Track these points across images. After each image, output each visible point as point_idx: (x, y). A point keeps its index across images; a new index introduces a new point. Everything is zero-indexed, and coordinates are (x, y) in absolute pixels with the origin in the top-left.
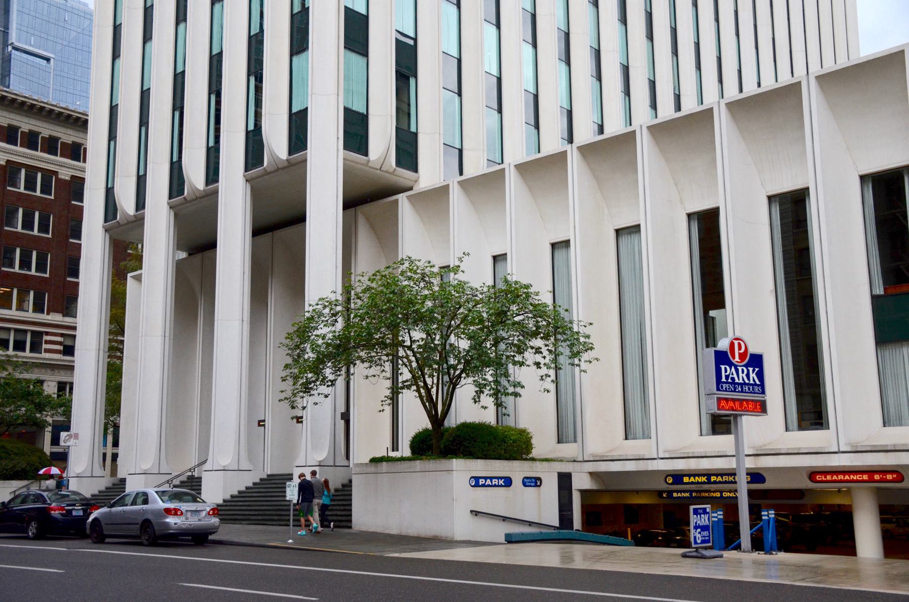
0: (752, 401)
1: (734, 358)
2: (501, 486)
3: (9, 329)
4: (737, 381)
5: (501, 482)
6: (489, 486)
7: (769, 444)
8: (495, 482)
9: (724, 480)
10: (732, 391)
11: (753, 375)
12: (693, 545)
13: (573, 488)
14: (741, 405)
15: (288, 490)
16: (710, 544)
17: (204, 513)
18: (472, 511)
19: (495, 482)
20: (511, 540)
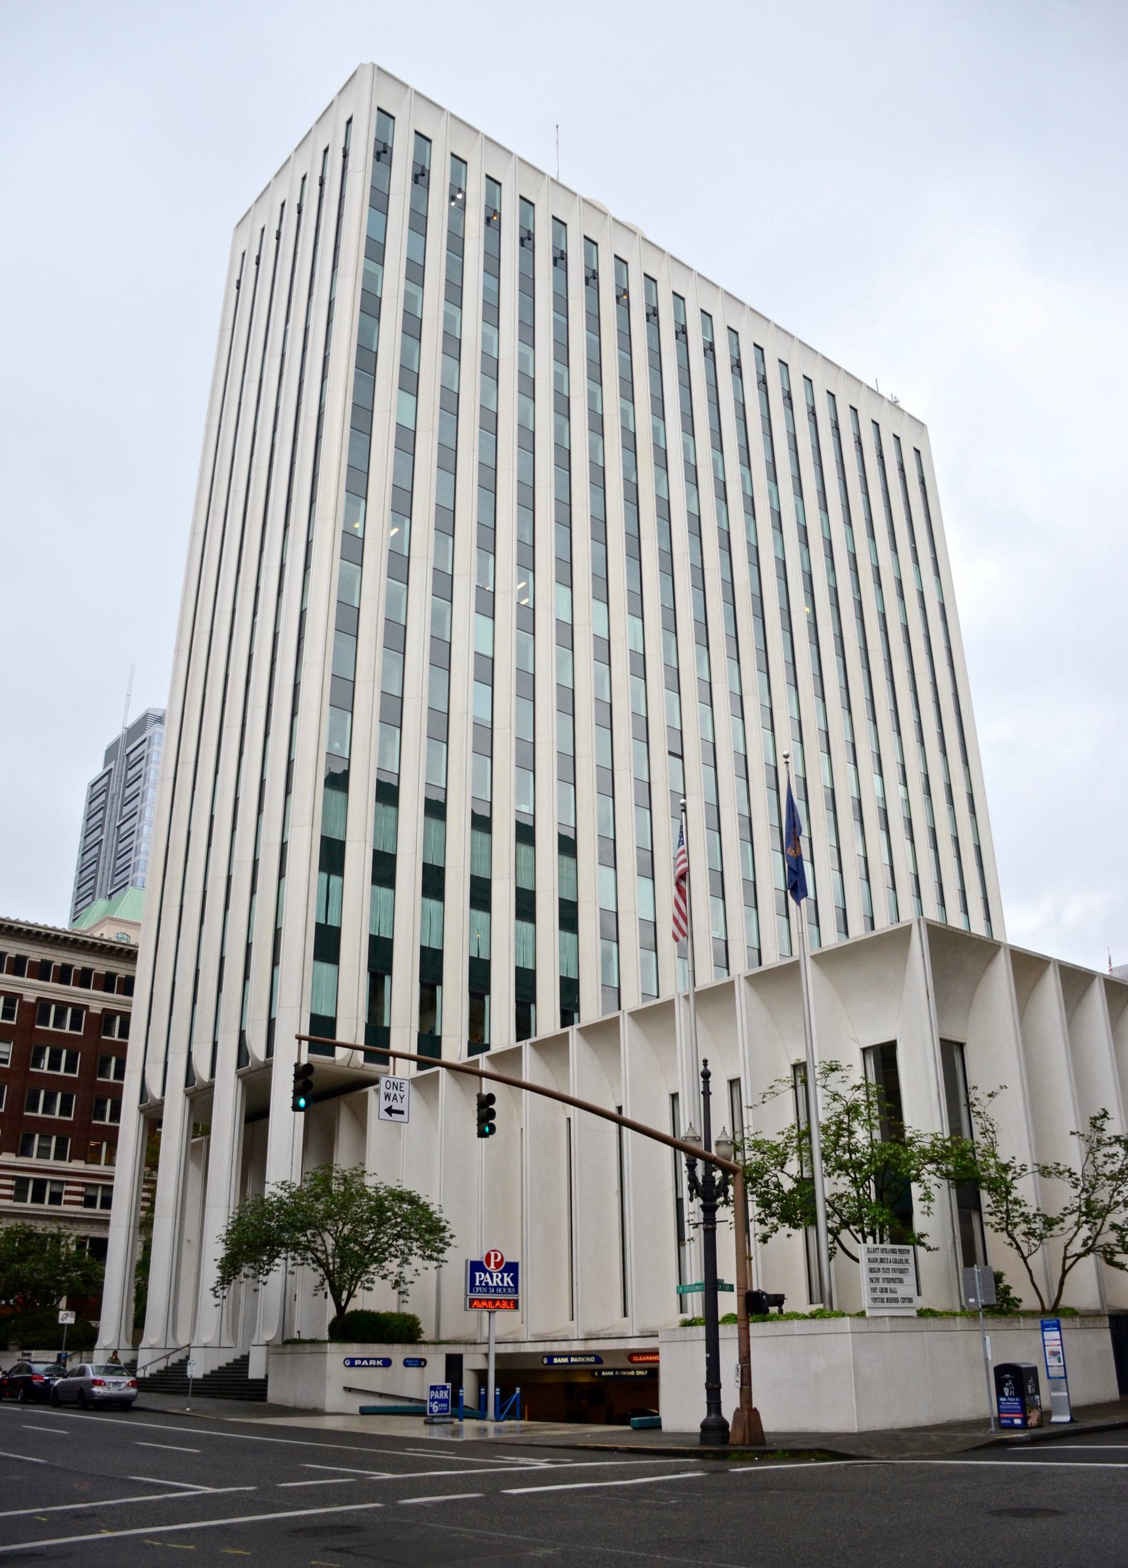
0: (505, 1300)
1: (489, 1265)
2: (379, 1366)
3: (97, 1186)
4: (490, 1284)
5: (379, 1363)
6: (365, 1366)
7: (608, 1328)
8: (372, 1362)
9: (371, 1363)
10: (485, 1293)
11: (507, 1279)
12: (428, 1414)
13: (464, 1367)
14: (494, 1304)
15: (189, 1367)
16: (449, 1413)
17: (123, 1385)
18: (345, 1388)
19: (372, 1362)
20: (365, 1411)
